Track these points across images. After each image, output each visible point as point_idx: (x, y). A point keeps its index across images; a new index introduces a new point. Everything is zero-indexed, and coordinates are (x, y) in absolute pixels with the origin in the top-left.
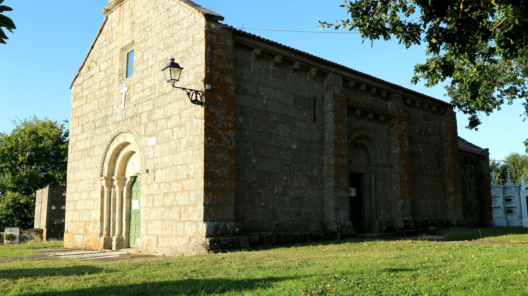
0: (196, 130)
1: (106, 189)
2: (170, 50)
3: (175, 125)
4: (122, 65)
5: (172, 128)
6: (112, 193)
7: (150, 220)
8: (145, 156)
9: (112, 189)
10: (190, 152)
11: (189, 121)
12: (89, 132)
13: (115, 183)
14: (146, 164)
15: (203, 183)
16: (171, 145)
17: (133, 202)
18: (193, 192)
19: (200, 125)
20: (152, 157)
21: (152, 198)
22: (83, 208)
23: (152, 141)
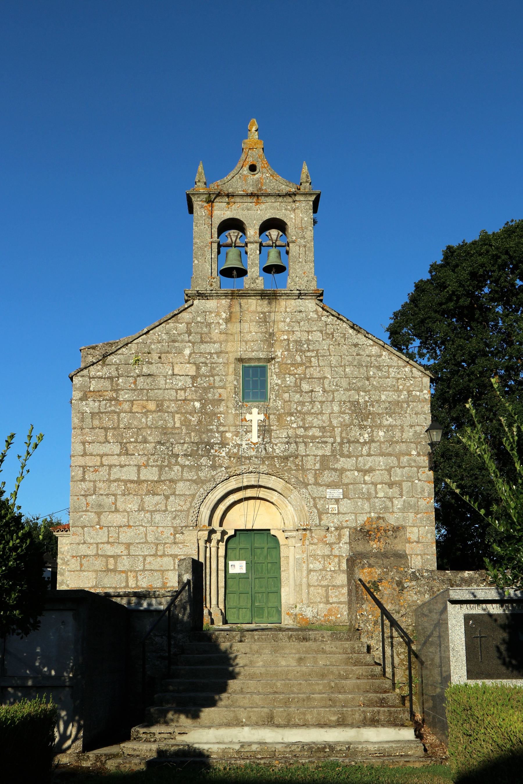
0: (420, 492)
1: (202, 544)
2: (362, 393)
3: (379, 481)
4: (238, 381)
5: (375, 484)
6: (208, 549)
7: (334, 586)
8: (318, 510)
9: (208, 545)
10: (412, 515)
11: (407, 481)
12: (152, 458)
13: (216, 537)
14: (320, 519)
15: (435, 548)
16: (374, 502)
17: (230, 563)
18: (419, 557)
19: (426, 489)
20: (336, 512)
21: (336, 560)
22: (141, 568)
23: (338, 493)
